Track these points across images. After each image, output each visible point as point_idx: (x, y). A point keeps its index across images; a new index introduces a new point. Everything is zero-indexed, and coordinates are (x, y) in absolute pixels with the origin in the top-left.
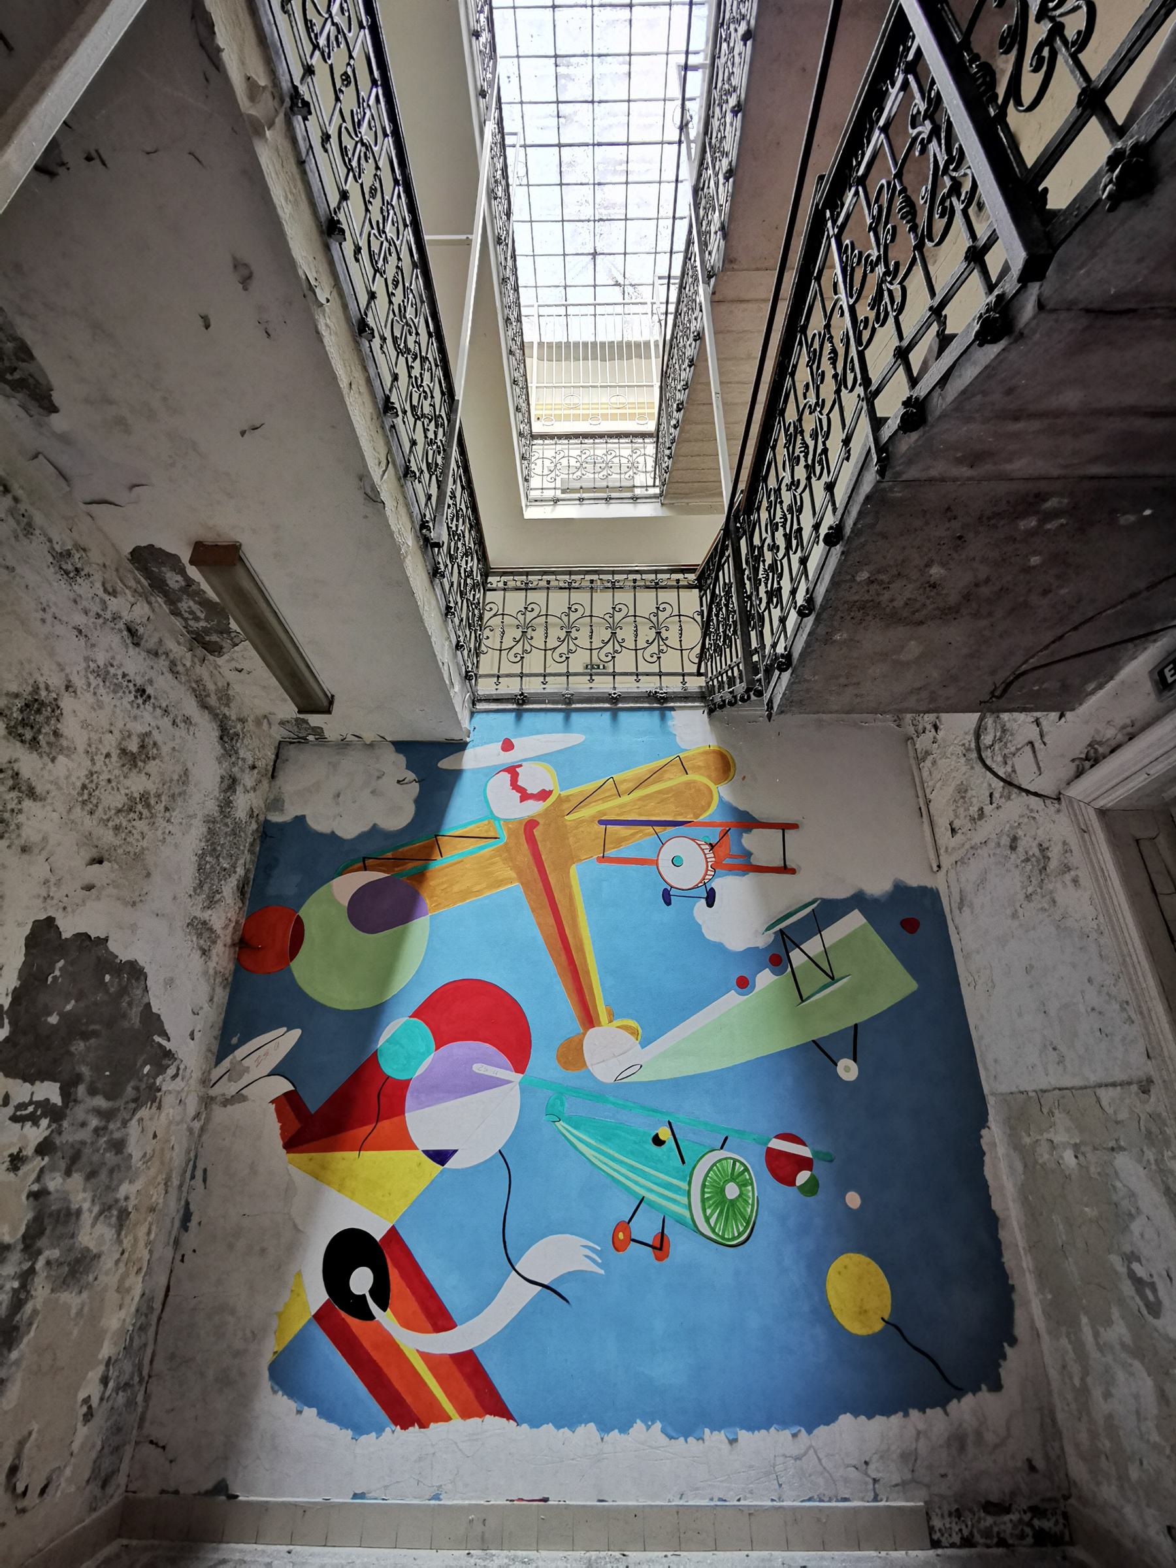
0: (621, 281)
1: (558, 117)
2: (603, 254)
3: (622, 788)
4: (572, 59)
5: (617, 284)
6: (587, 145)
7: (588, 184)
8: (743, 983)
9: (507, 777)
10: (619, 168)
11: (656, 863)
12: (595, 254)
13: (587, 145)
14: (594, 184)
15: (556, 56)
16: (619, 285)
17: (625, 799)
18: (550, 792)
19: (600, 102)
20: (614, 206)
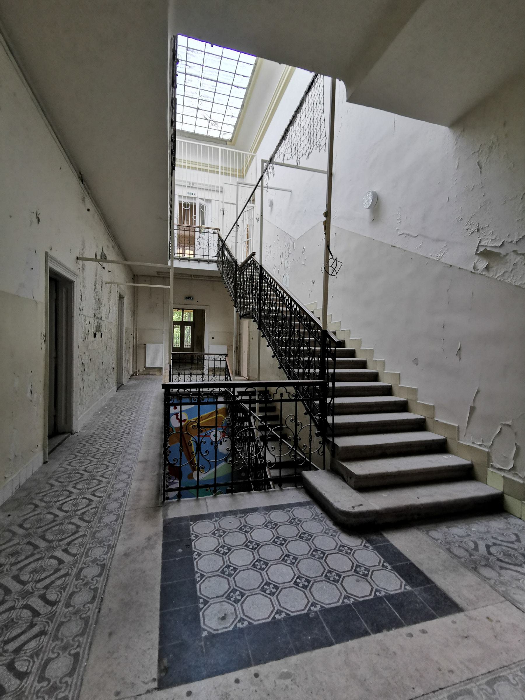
0: (209, 119)
1: (186, 65)
2: (201, 110)
3: (203, 418)
4: (195, 51)
5: (206, 119)
6: (199, 77)
7: (197, 88)
8: (226, 460)
9: (175, 416)
10: (212, 87)
11: (210, 436)
12: (198, 109)
13: (199, 77)
14: (200, 89)
15: (187, 47)
16: (208, 120)
17: (204, 421)
18: (186, 420)
19: (206, 66)
20: (208, 97)
